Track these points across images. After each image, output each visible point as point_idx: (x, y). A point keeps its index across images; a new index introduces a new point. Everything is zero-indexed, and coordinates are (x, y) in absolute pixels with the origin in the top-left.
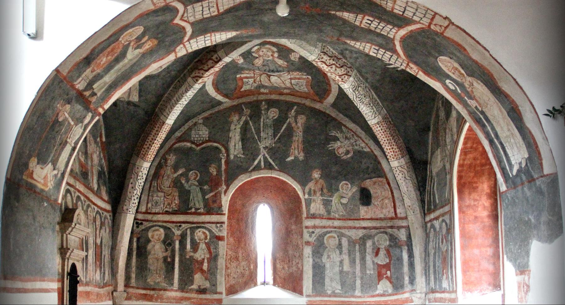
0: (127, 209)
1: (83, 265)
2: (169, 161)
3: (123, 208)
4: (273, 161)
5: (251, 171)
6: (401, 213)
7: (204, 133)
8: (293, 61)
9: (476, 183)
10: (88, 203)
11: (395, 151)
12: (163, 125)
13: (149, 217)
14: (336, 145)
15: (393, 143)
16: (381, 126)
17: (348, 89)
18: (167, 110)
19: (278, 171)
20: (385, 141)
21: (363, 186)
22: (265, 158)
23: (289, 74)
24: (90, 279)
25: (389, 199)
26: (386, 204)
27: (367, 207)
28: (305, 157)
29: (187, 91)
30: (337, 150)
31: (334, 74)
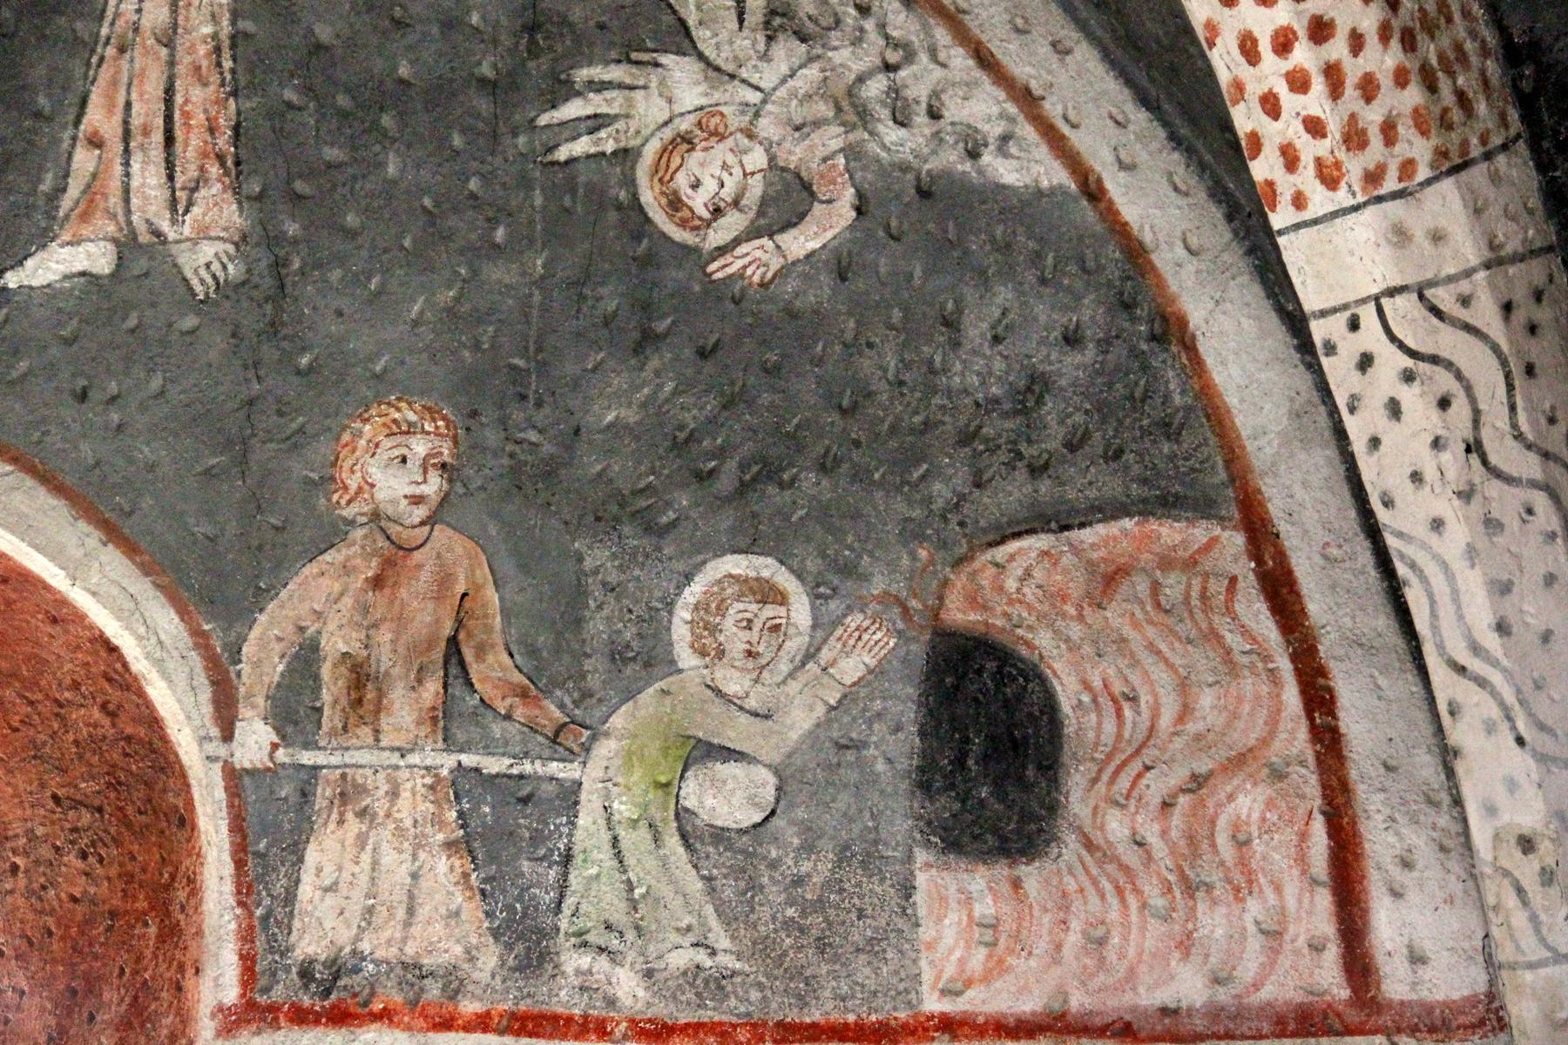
6: (1417, 959)
14: (649, 109)
21: (958, 614)
25: (1278, 775)
26: (1242, 844)
27: (1002, 870)
30: (663, 171)
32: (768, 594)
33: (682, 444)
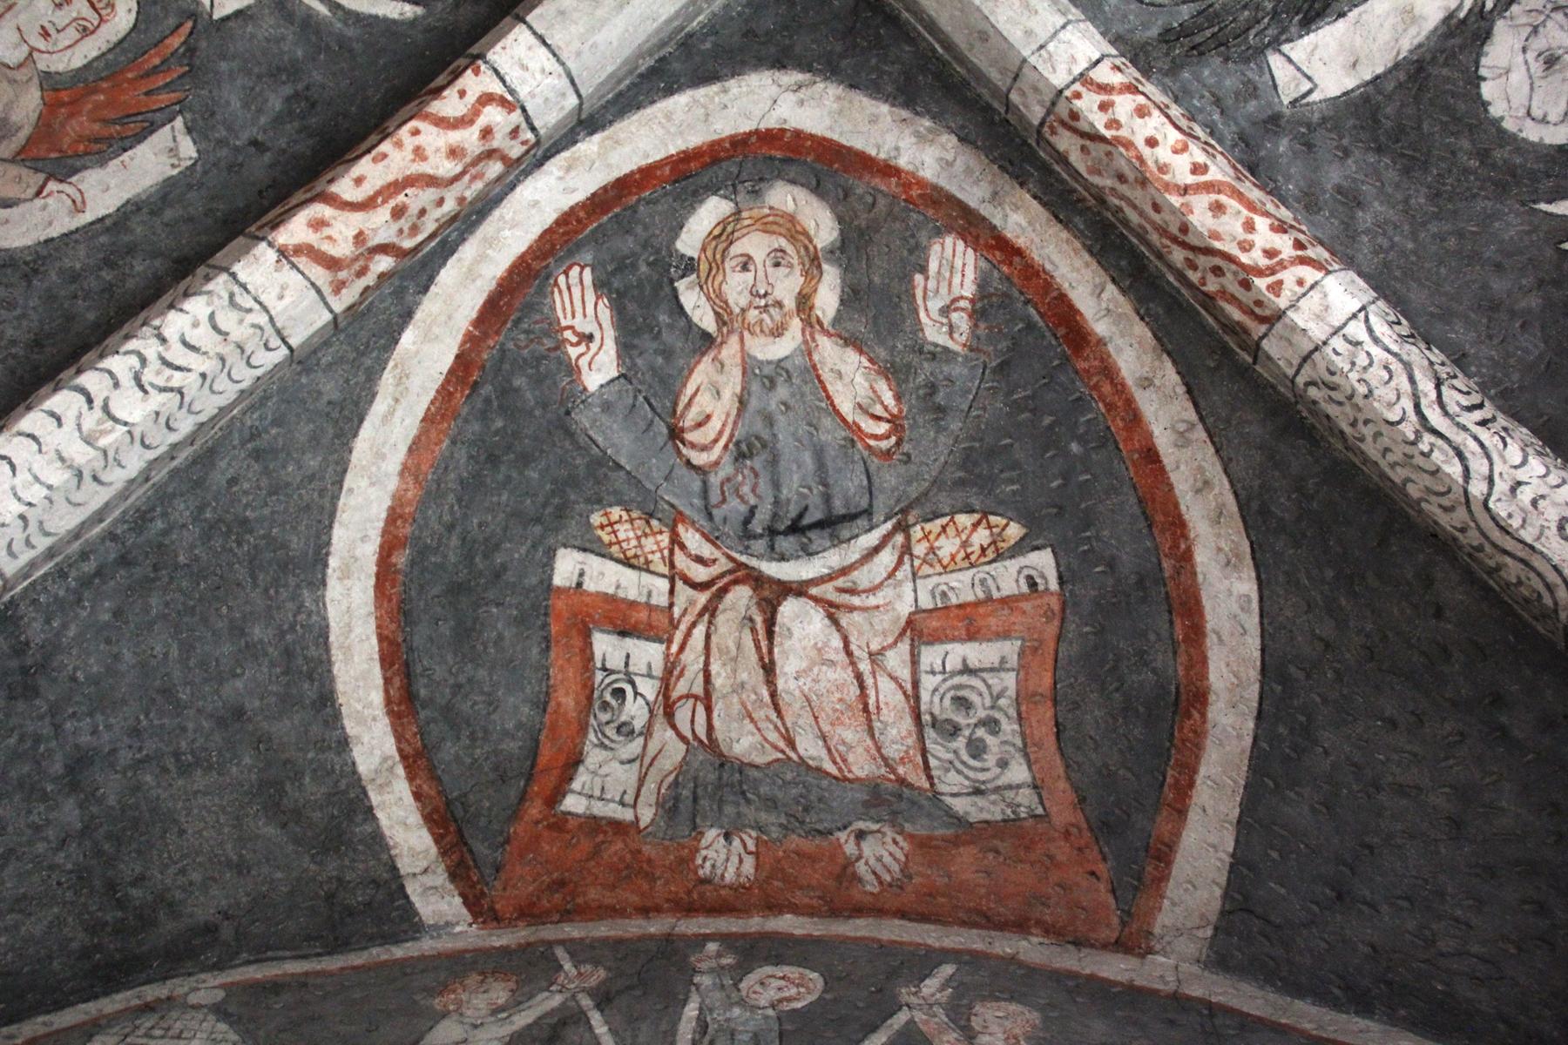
17: (1357, 330)
31: (1232, 204)
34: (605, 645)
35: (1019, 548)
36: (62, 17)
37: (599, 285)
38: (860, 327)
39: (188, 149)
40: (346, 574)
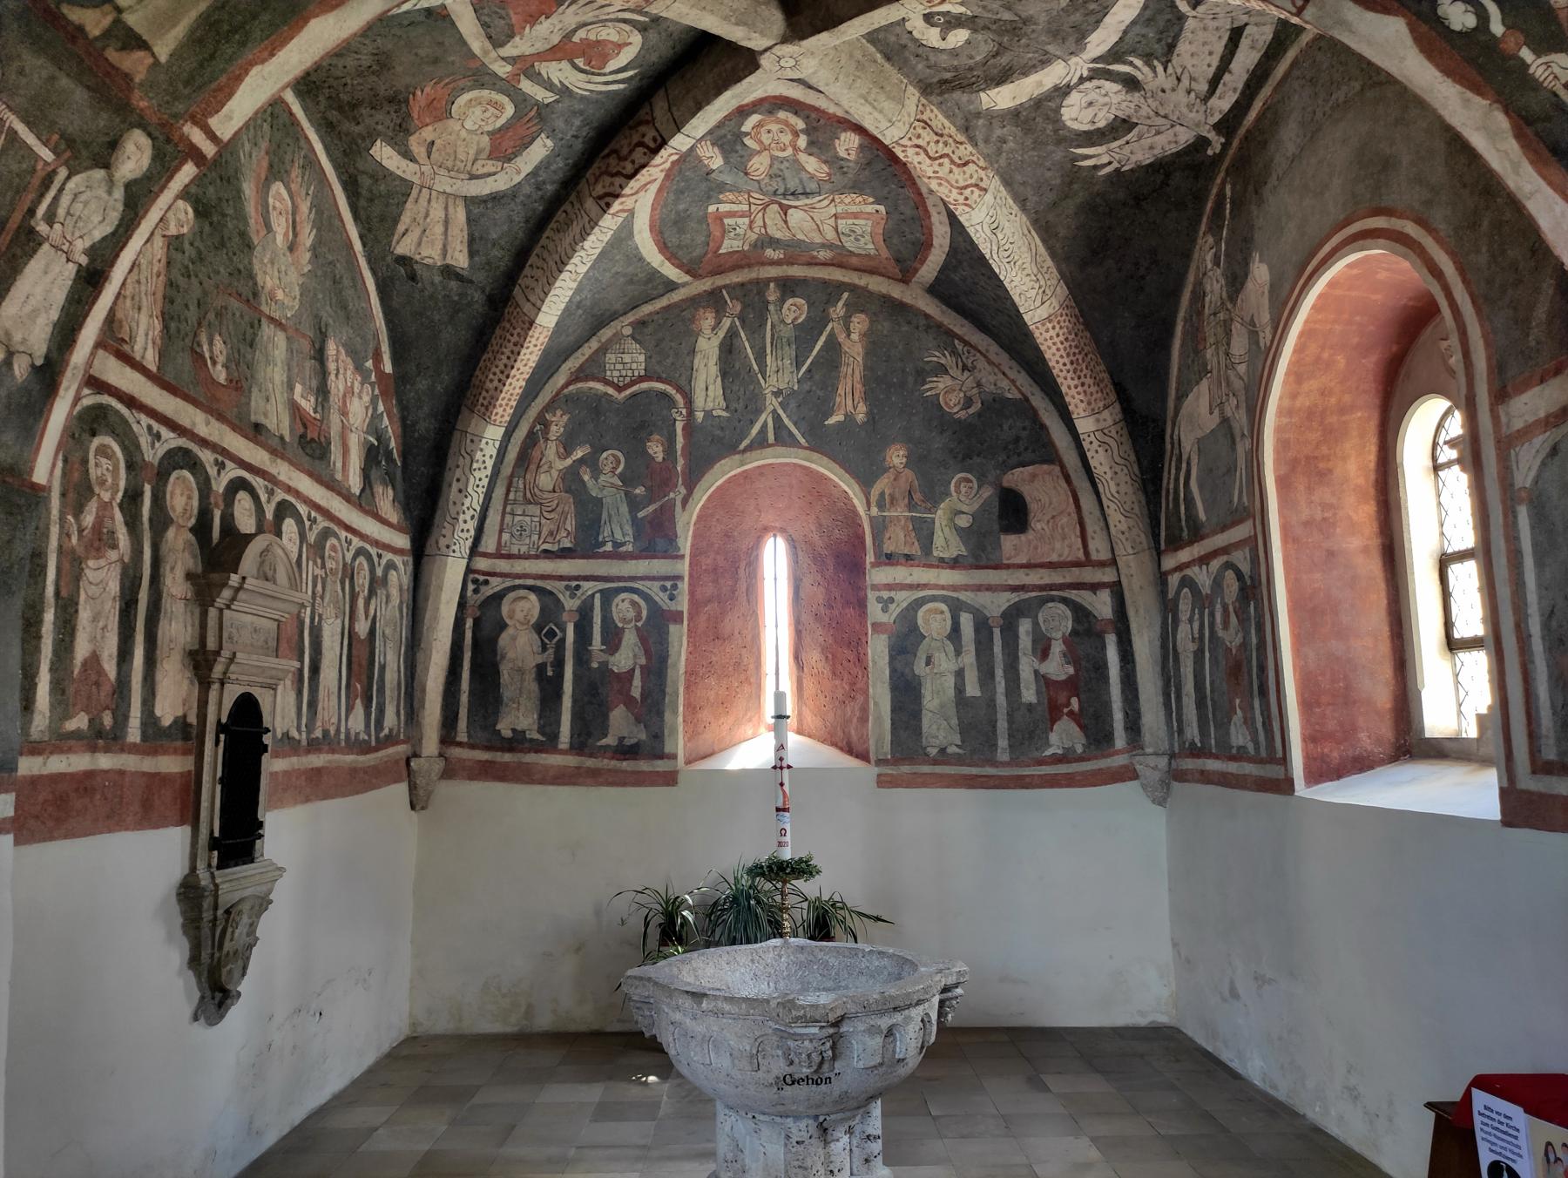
0: (448, 547)
1: (299, 693)
2: (553, 428)
3: (437, 543)
4: (795, 424)
5: (744, 451)
7: (634, 359)
8: (842, 159)
9: (1327, 458)
10: (323, 523)
11: (1089, 391)
12: (529, 329)
13: (503, 565)
14: (941, 386)
15: (1085, 371)
16: (1058, 327)
17: (979, 227)
18: (538, 290)
19: (806, 448)
20: (1065, 364)
21: (1005, 484)
22: (777, 419)
23: (833, 200)
24: (326, 733)
28: (869, 414)
29: (584, 235)
32: (969, 481)
33: (951, 451)
34: (726, 221)
35: (873, 203)
36: (487, 114)
37: (713, 144)
38: (815, 150)
39: (549, 143)
40: (640, 232)
